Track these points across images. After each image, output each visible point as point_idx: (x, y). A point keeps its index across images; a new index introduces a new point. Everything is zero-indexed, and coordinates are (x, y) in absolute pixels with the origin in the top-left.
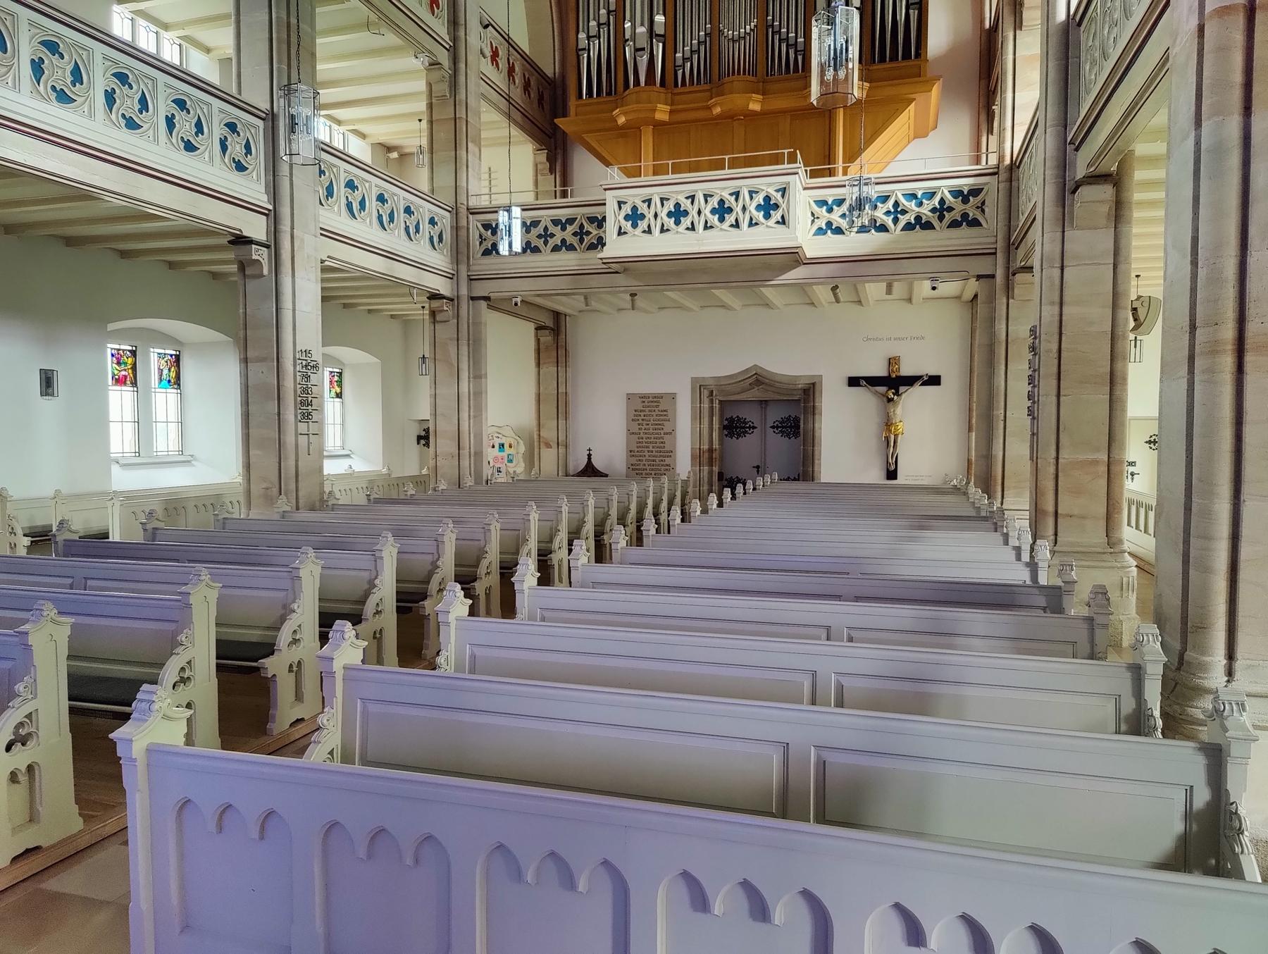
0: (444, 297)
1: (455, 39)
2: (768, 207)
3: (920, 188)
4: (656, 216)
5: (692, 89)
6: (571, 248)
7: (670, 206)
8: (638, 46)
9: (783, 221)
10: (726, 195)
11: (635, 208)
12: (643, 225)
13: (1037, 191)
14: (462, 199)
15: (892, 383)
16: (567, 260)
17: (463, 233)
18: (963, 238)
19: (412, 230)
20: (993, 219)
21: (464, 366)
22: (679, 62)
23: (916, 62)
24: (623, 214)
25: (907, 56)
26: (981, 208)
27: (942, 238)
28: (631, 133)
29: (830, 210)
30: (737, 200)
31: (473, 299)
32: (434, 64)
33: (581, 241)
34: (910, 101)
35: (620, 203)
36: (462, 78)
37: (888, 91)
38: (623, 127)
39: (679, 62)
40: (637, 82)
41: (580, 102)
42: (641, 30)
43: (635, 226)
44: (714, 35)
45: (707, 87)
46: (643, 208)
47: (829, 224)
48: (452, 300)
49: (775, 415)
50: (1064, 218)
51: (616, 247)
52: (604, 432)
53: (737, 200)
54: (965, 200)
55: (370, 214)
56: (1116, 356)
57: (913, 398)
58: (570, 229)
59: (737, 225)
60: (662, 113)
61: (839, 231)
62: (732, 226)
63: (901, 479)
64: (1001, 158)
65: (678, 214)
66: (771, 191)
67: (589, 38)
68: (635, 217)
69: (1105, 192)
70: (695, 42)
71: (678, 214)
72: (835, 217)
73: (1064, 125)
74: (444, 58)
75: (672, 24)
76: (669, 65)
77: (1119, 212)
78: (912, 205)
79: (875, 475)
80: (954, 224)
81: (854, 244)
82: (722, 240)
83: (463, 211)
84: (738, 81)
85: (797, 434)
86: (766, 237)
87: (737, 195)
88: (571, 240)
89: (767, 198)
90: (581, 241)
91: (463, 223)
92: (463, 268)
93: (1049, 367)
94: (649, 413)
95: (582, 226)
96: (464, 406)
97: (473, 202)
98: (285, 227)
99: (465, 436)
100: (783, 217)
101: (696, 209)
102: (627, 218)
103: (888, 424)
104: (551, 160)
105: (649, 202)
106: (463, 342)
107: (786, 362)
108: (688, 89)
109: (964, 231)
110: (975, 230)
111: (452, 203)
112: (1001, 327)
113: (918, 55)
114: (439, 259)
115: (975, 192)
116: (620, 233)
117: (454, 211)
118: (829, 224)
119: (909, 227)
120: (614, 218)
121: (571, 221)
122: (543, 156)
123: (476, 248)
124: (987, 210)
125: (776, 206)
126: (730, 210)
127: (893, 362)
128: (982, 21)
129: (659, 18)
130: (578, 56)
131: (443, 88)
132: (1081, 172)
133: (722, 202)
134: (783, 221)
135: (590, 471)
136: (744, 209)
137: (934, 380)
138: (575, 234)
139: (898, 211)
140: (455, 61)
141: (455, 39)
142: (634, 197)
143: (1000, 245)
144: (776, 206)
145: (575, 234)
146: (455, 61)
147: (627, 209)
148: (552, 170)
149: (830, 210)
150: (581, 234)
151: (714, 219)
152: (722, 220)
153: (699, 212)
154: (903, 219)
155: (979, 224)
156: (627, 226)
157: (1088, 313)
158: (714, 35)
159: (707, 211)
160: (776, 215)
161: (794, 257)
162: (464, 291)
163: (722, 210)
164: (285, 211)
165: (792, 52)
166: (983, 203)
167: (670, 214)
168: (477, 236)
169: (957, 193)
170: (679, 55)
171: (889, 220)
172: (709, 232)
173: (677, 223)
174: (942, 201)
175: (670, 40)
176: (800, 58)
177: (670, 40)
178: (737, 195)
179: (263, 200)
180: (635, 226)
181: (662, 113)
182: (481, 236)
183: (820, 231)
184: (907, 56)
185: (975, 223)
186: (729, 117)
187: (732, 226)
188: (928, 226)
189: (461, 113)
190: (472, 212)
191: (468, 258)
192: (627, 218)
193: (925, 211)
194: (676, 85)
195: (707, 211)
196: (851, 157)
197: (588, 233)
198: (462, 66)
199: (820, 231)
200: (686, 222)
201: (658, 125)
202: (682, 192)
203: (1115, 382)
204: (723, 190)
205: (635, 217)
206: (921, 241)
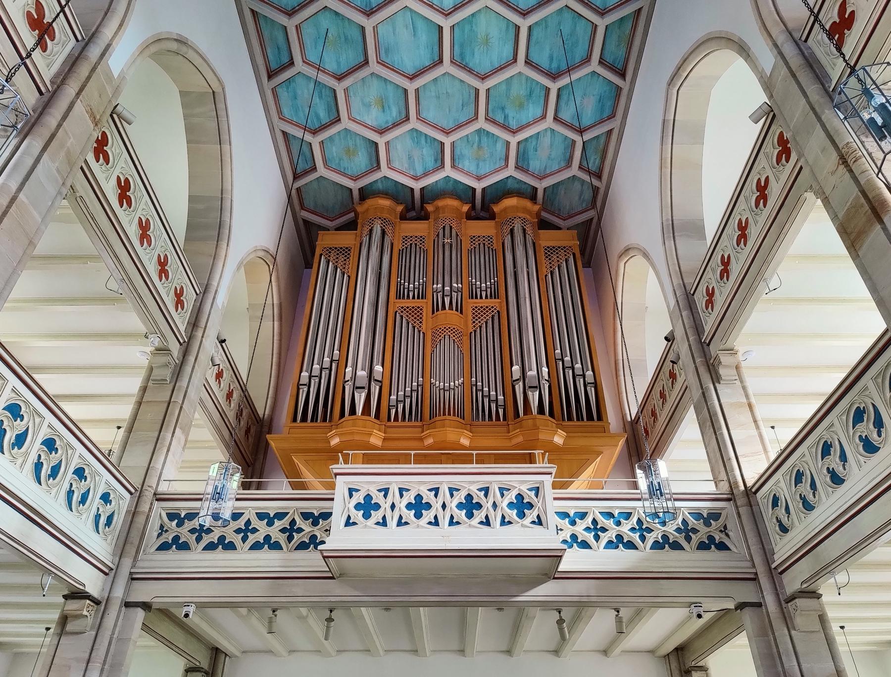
0: (88, 597)
1: (190, 338)
4: (393, 506)
5: (403, 424)
6: (276, 546)
7: (409, 497)
8: (357, 385)
9: (539, 522)
10: (474, 489)
11: (368, 497)
14: (152, 481)
17: (140, 520)
19: (76, 497)
22: (393, 403)
23: (600, 423)
24: (354, 502)
29: (573, 523)
30: (486, 495)
31: (128, 605)
32: (162, 350)
33: (290, 539)
34: (599, 453)
35: (351, 491)
36: (188, 369)
37: (580, 442)
38: (337, 445)
39: (393, 403)
40: (353, 411)
41: (294, 424)
42: (362, 374)
43: (367, 516)
45: (419, 424)
46: (378, 498)
47: (574, 537)
48: (97, 602)
51: (339, 538)
53: (486, 495)
54: (707, 524)
55: (27, 454)
58: (278, 524)
59: (487, 522)
62: (481, 523)
64: (732, 486)
65: (419, 506)
66: (524, 488)
68: (368, 507)
70: (408, 389)
74: (175, 348)
76: (384, 404)
80: (702, 546)
83: (149, 495)
87: (486, 491)
90: (290, 539)
91: (145, 507)
92: (127, 563)
95: (293, 522)
97: (163, 488)
100: (538, 517)
101: (440, 503)
102: (358, 507)
108: (400, 423)
111: (137, 481)
113: (600, 418)
114: (100, 546)
115: (715, 515)
116: (349, 523)
117: (138, 494)
118: (574, 537)
119: (657, 546)
120: (341, 506)
121: (280, 516)
123: (152, 538)
124: (730, 534)
125: (530, 506)
126: (479, 506)
128: (624, 417)
130: (298, 389)
131: (167, 374)
133: (469, 497)
136: (495, 505)
138: (283, 531)
139: (642, 529)
140: (185, 353)
141: (190, 338)
142: (369, 485)
143: (761, 569)
144: (530, 506)
145: (283, 531)
146: (185, 353)
147: (359, 498)
149: (573, 523)
150: (291, 530)
152: (470, 515)
153: (444, 506)
154: (651, 538)
155: (727, 548)
160: (531, 515)
162: (119, 593)
163: (470, 506)
165: (493, 406)
166: (725, 527)
167: (409, 506)
168: (157, 527)
169: (698, 515)
170: (393, 397)
171: (636, 537)
172: (454, 528)
173: (418, 516)
174: (684, 522)
176: (501, 411)
178: (486, 491)
180: (367, 516)
181: (376, 439)
182: (162, 527)
184: (590, 417)
185: (722, 547)
187: (481, 523)
188: (676, 546)
189: (178, 397)
190: (159, 498)
191: (137, 552)
192: (358, 507)
193: (670, 528)
194: (389, 419)
197: (300, 530)
198: (191, 359)
200: (428, 516)
202: (424, 483)
205: (368, 507)
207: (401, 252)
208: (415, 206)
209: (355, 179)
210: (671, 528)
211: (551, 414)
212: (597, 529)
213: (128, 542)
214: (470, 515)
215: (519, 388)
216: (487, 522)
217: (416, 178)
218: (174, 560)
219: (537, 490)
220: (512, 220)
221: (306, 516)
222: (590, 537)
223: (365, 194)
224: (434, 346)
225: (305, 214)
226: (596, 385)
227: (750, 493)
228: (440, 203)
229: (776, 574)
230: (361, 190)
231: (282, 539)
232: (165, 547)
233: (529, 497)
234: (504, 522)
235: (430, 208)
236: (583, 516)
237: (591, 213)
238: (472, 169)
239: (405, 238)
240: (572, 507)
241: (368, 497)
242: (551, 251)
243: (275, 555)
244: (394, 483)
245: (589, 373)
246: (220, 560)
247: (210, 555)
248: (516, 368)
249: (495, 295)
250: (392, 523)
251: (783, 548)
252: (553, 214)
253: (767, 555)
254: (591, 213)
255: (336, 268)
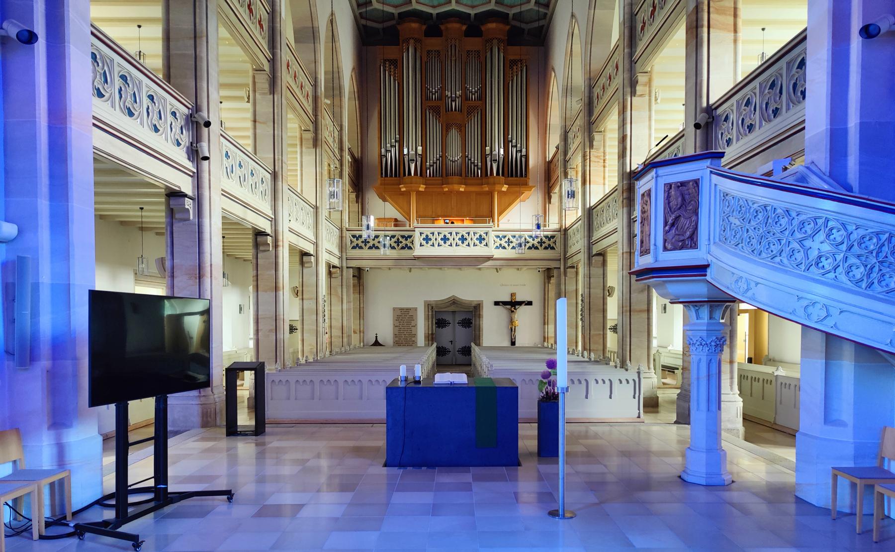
1: (341, 156)
2: (481, 239)
3: (533, 234)
7: (442, 236)
9: (487, 245)
10: (464, 233)
11: (427, 236)
12: (430, 243)
13: (578, 243)
15: (513, 304)
16: (394, 254)
18: (549, 253)
20: (559, 246)
21: (345, 297)
25: (521, 175)
26: (555, 243)
27: (541, 253)
28: (407, 194)
35: (421, 234)
37: (516, 189)
43: (427, 243)
44: (443, 156)
46: (430, 236)
49: (459, 318)
50: (590, 264)
51: (418, 251)
52: (382, 325)
56: (604, 303)
57: (522, 310)
59: (469, 245)
60: (422, 188)
61: (504, 248)
63: (517, 345)
65: (445, 239)
67: (386, 151)
68: (427, 239)
69: (601, 258)
71: (445, 239)
72: (503, 242)
73: (590, 236)
75: (425, 150)
77: (604, 263)
78: (531, 240)
79: (507, 343)
80: (546, 248)
81: (509, 253)
82: (462, 251)
83: (344, 229)
84: (456, 178)
85: (469, 327)
86: (479, 251)
87: (469, 233)
88: (394, 245)
89: (480, 236)
92: (344, 254)
93: (587, 307)
94: (404, 317)
96: (345, 315)
98: (320, 249)
99: (345, 329)
102: (424, 239)
103: (511, 321)
104: (357, 197)
105: (433, 234)
106: (344, 287)
107: (467, 295)
109: (549, 251)
110: (552, 251)
112: (563, 287)
114: (336, 252)
115: (553, 237)
117: (341, 230)
119: (530, 248)
120: (418, 239)
122: (353, 196)
127: (513, 295)
128: (545, 158)
129: (420, 148)
132: (594, 253)
134: (487, 245)
135: (377, 343)
137: (530, 303)
141: (341, 156)
142: (427, 231)
143: (562, 257)
147: (424, 236)
148: (357, 202)
150: (398, 242)
151: (460, 242)
156: (424, 243)
157: (597, 292)
158: (443, 156)
159: (457, 239)
160: (484, 243)
161: (489, 258)
164: (320, 243)
169: (546, 237)
175: (424, 157)
177: (424, 157)
178: (469, 233)
179: (313, 239)
181: (422, 188)
183: (497, 248)
184: (521, 175)
185: (553, 248)
186: (450, 192)
188: (537, 248)
192: (424, 239)
193: (535, 242)
195: (457, 239)
196: (500, 214)
199: (497, 248)
200: (448, 243)
201: (419, 193)
203: (604, 311)
204: (463, 232)
205: (427, 239)
206: (534, 254)
207: (426, 63)
208: (433, 25)
209: (396, 7)
210: (536, 240)
211: (503, 175)
212: (509, 242)
213: (342, 247)
214: (463, 243)
215: (488, 159)
216: (469, 245)
217: (434, 7)
218: (357, 253)
219: (487, 233)
220: (492, 39)
221: (403, 237)
222: (506, 245)
223: (404, 17)
224: (447, 131)
225: (363, 22)
226: (527, 157)
227: (566, 230)
228: (450, 25)
229: (566, 259)
230: (399, 14)
231: (395, 245)
232: (354, 248)
233: (484, 236)
234: (475, 245)
235: (442, 27)
236: (505, 237)
237: (542, 23)
238: (469, 3)
239: (428, 52)
240: (501, 234)
241: (427, 236)
242: (513, 63)
243: (394, 251)
244: (436, 231)
245: (524, 150)
246: (374, 253)
247: (370, 251)
248: (488, 148)
249: (480, 100)
250: (436, 245)
251: (571, 251)
252: (521, 22)
253: (565, 252)
254: (542, 23)
255: (390, 76)
